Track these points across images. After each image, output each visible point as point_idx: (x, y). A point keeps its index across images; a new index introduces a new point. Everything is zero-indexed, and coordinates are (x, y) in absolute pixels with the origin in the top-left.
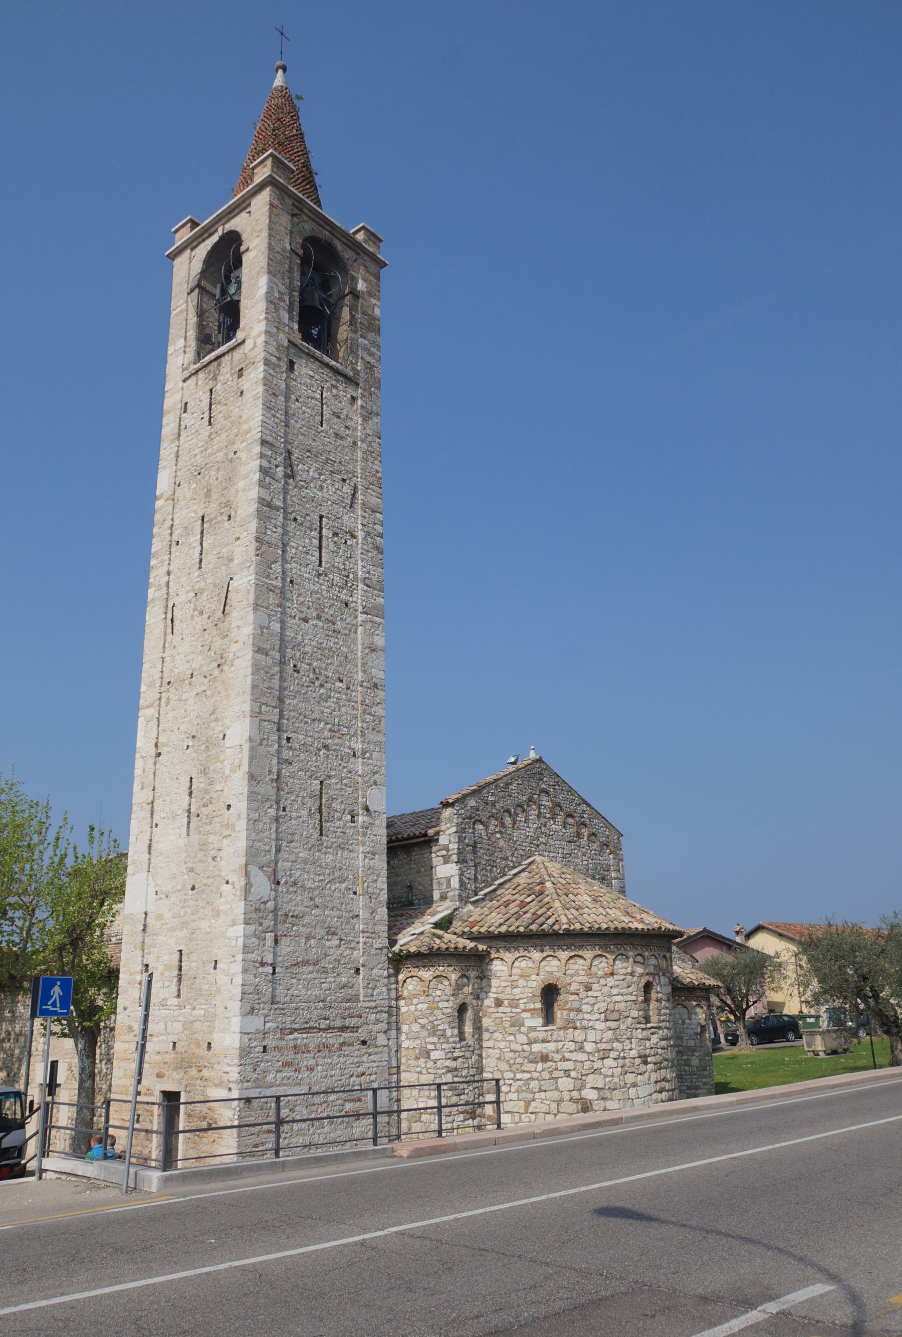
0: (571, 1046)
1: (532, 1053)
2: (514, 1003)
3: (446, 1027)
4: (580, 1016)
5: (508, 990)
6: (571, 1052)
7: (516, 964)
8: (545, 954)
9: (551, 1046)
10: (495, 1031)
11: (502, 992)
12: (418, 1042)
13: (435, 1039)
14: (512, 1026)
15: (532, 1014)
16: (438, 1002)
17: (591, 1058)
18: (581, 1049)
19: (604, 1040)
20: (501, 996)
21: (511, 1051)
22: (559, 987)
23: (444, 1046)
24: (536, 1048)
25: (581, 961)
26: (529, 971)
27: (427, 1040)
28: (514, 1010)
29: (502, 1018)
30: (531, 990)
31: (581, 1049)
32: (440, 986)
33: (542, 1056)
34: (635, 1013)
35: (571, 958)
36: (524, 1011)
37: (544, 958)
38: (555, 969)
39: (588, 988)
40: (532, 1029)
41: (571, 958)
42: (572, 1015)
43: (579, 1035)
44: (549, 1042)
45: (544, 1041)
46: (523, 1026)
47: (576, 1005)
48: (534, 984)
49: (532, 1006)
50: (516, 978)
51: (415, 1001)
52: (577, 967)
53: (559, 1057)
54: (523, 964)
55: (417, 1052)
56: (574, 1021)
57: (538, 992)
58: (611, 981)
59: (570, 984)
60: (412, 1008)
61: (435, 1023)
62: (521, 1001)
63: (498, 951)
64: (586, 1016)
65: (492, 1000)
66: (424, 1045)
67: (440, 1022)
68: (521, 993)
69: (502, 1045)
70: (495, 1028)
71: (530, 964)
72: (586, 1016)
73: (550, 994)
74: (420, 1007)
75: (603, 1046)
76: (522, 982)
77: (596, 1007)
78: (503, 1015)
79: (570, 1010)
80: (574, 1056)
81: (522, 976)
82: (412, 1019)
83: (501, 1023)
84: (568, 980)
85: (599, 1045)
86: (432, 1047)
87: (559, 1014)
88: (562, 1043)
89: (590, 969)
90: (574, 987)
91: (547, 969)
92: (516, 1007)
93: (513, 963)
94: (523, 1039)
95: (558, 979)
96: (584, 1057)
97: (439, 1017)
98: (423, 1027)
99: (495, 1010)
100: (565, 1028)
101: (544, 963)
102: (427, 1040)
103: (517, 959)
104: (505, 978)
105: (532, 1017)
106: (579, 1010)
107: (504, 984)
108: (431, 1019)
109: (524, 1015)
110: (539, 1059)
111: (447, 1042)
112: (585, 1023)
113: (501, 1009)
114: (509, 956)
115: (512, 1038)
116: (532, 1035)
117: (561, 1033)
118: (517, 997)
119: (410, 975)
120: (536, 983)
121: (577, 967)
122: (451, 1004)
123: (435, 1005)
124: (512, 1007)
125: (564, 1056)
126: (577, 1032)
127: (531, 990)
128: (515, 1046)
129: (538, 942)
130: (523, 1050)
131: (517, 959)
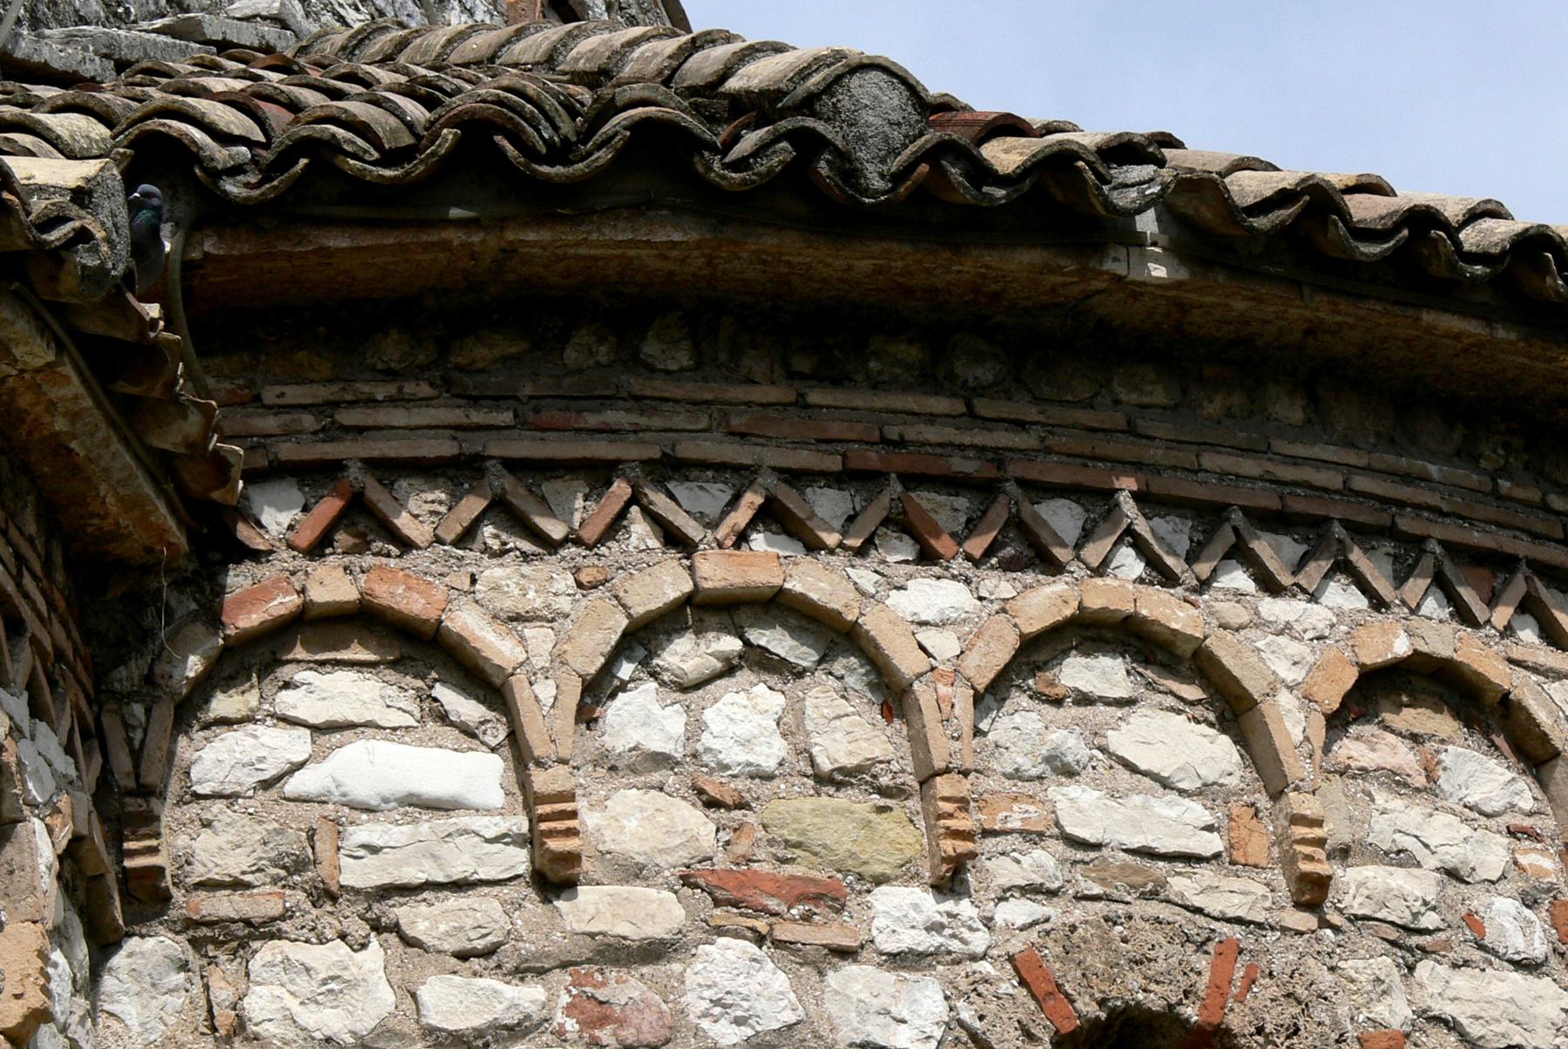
8: (1045, 601)
37: (1038, 651)
38: (1178, 824)
50: (657, 911)
52: (1445, 835)
54: (744, 723)
63: (365, 524)
71: (846, 729)
81: (724, 896)
91: (1082, 807)
93: (598, 690)
103: (644, 637)
104: (481, 915)
114: (523, 604)
129: (930, 421)
131: (644, 637)
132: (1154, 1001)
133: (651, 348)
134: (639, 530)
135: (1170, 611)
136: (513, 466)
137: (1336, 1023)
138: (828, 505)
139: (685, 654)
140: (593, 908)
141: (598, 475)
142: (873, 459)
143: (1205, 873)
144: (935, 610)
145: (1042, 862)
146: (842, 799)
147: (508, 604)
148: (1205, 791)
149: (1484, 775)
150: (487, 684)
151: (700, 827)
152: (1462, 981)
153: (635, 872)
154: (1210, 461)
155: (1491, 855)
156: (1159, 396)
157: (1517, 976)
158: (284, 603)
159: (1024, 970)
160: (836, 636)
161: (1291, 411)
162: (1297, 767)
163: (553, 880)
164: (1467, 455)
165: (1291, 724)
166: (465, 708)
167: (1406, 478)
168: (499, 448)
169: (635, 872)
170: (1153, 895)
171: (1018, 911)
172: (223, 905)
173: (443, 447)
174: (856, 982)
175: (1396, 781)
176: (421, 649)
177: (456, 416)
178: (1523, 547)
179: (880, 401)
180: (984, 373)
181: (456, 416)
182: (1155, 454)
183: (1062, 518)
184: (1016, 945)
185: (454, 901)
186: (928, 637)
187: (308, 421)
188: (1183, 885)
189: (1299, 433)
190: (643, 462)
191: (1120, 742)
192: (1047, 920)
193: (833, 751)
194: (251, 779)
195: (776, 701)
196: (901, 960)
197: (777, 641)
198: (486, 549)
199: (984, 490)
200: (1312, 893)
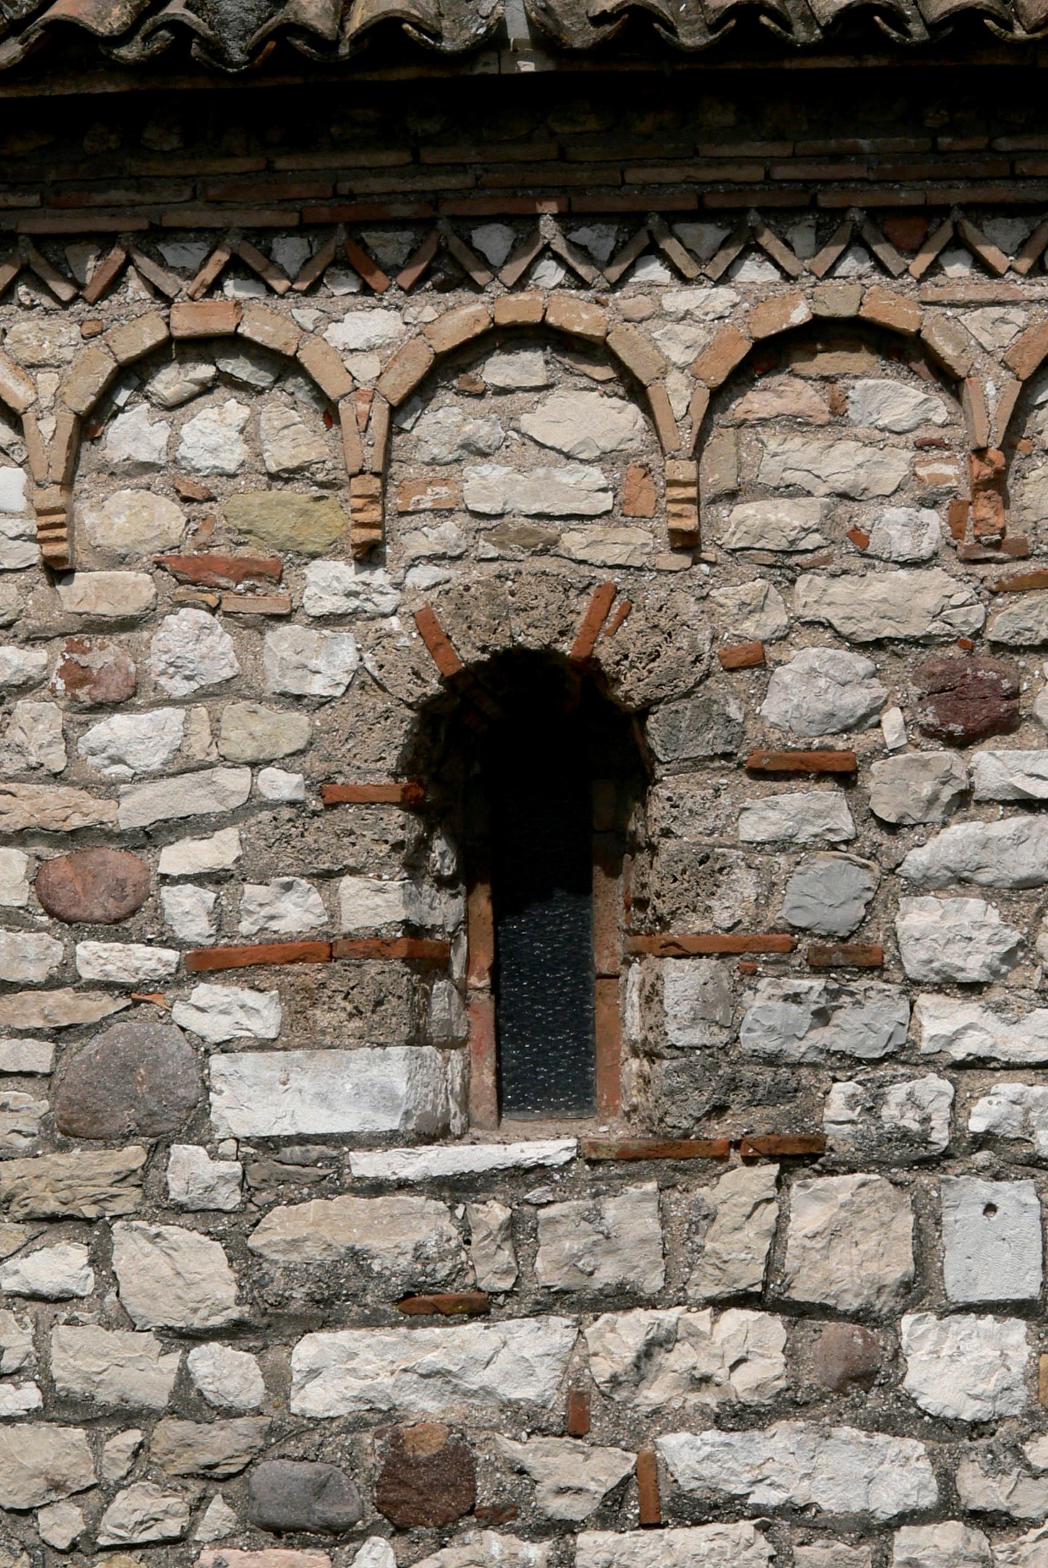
0: (752, 1351)
1: (283, 1431)
4: (867, 1020)
6: (739, 1417)
7: (134, 433)
8: (461, 316)
9: (518, 1358)
14: (66, 1131)
15: (300, 1006)
17: (978, 1488)
18: (862, 1387)
21: (61, 1407)
22: (632, 687)
24: (340, 1371)
25: (897, 399)
26: (282, 513)
28: (96, 957)
30: (296, 727)
31: (862, 1387)
33: (398, 1468)
35: (771, 355)
36: (204, 964)
37: (452, 366)
38: (580, 487)
41: (771, 355)
42: (772, 1014)
43: (841, 1235)
44: (479, 1308)
45: (425, 1301)
46: (195, 1124)
47: (823, 895)
48: (331, 664)
49: (296, 912)
50: (136, 588)
52: (841, 462)
53: (601, 1468)
54: (214, 433)
56: (785, 1079)
57: (377, 753)
59: (755, 662)
62: (175, 858)
64: (942, 1021)
68: (182, 766)
71: (290, 433)
72: (942, 1021)
73: (529, 779)
79: (748, 952)
80: (779, 1463)
81: (190, 575)
84: (744, 606)
87: (659, 1002)
88: (623, 1334)
89: (996, 485)
90: (808, 690)
91: (488, 485)
92: (114, 928)
93: (90, 424)
94: (181, 1271)
95: (610, 602)
96: (899, 1475)
100: (673, 1156)
101: (445, 420)
103: (134, 372)
105: (299, 1034)
106: (851, 958)
109: (217, 1009)
110: (353, 1501)
112: (920, 1101)
115: (60, 1265)
116: (302, 1231)
117: (633, 1211)
118: (137, 809)
120: (345, 650)
121: (841, 462)
124: (70, 923)
125: (650, 1467)
126: (815, 1204)
127: (296, 727)
128: (84, 1356)
129: (378, 173)
130: (188, 1402)
131: (134, 372)
132: (533, 640)
133: (150, 134)
134: (134, 286)
135: (579, 315)
136: (39, 241)
137: (693, 646)
138: (289, 251)
139: (169, 381)
140: (85, 593)
141: (105, 241)
142: (324, 214)
143: (596, 529)
144: (364, 334)
146: (287, 492)
147: (26, 355)
152: (840, 588)
153: (120, 561)
154: (632, 176)
156: (592, 124)
157: (903, 574)
159: (425, 623)
160: (285, 366)
163: (58, 571)
167: (836, 158)
168: (27, 226)
170: (544, 552)
171: (423, 576)
174: (282, 641)
179: (336, 162)
180: (431, 126)
182: (582, 176)
183: (493, 240)
184: (418, 605)
186: (354, 363)
188: (574, 541)
190: (134, 232)
191: (533, 423)
192: (447, 582)
193: (280, 454)
195: (245, 412)
196: (324, 620)
197: (240, 368)
198: (21, 305)
199: (424, 225)
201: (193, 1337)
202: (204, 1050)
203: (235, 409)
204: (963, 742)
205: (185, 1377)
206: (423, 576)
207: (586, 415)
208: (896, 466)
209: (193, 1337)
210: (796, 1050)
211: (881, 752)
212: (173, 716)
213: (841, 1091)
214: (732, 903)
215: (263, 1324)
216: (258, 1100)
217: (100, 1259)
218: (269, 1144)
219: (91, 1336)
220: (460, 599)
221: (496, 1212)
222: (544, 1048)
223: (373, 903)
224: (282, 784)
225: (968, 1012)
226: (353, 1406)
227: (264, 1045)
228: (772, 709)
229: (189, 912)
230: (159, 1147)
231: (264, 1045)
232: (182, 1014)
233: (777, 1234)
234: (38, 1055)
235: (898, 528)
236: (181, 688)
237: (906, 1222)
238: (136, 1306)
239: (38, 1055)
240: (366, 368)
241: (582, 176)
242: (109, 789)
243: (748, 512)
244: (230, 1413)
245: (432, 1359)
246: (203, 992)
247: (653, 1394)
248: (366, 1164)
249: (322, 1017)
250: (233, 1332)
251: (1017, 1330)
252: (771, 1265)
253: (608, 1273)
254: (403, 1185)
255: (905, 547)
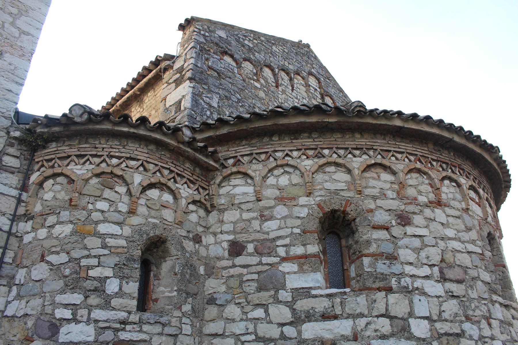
2: (266, 247)
3: (109, 272)
4: (397, 268)
5: (256, 224)
7: (271, 180)
10: (228, 302)
11: (245, 230)
12: (36, 302)
13: (77, 298)
14: (260, 289)
15: (301, 266)
16: (97, 223)
19: (445, 315)
20: (242, 238)
22: (352, 214)
23: (98, 314)
26: (294, 191)
27: (60, 299)
28: (265, 260)
29: (241, 275)
32: (107, 193)
34: (486, 277)
35: (369, 167)
36: (284, 259)
38: (341, 186)
39: (404, 220)
40: (304, 293)
41: (369, 167)
42: (382, 267)
43: (398, 304)
44: (336, 317)
45: (326, 317)
46: (283, 287)
48: (304, 212)
49: (299, 250)
50: (272, 203)
51: (51, 220)
52: (380, 184)
54: (284, 181)
55: (30, 323)
56: (384, 277)
58: (439, 214)
60: (42, 233)
61: (84, 262)
62: (279, 243)
64: (408, 269)
65: (225, 245)
66: (48, 309)
67: (94, 262)
68: (280, 228)
69: (239, 328)
70: (229, 297)
72: (408, 269)
74: (58, 229)
75: (442, 327)
76: (281, 211)
77: (423, 254)
78: (245, 271)
81: (281, 200)
82: (37, 256)
83: (241, 285)
85: (438, 325)
86: (67, 314)
88: (362, 322)
91: (328, 185)
92: (269, 255)
93: (265, 178)
95: (348, 202)
97: (94, 252)
98: (55, 269)
99: (229, 263)
102: (60, 299)
103: (271, 170)
104: (250, 206)
105: (301, 270)
107: (246, 216)
108: (76, 254)
109: (287, 267)
111: (107, 305)
112: (406, 281)
113: (240, 260)
114: (256, 169)
115: (259, 313)
117: (362, 299)
118: (272, 236)
119: (50, 172)
121: (380, 184)
122: (127, 231)
123: (90, 228)
126: (392, 298)
127: (298, 222)
131: (271, 170)
133: (274, 138)
136: (257, 154)
137: (362, 208)
139: (276, 172)
142: (300, 148)
143: (345, 192)
145: (322, 193)
146: (296, 187)
147: (254, 169)
148: (345, 182)
149: (386, 176)
150: (252, 178)
151: (278, 192)
152: (383, 202)
153: (269, 199)
154: (346, 143)
155: (388, 186)
156: (340, 136)
157: (391, 201)
158: (229, 172)
159: (319, 206)
160: (295, 168)
161: (358, 136)
162: (357, 178)
164: (384, 139)
165: (356, 172)
166: (249, 181)
168: (255, 152)
169: (269, 199)
170: (337, 195)
172: (221, 207)
173: (249, 152)
175: (374, 179)
176: (246, 175)
177: (250, 149)
178: (392, 149)
179: (302, 141)
180: (316, 136)
181: (250, 149)
182: (338, 143)
184: (318, 203)
185: (247, 204)
186: (306, 167)
187: (234, 152)
188: (342, 193)
189: (361, 138)
191: (333, 177)
193: (294, 181)
194: (225, 192)
195: (288, 177)
196: (302, 206)
200: (360, 192)
201: (282, 325)
202: (284, 274)
203: (287, 177)
204: (404, 226)
205: (282, 332)
206: (318, 199)
207: (342, 176)
208: (388, 186)
209: (282, 325)
210: (385, 272)
211: (393, 226)
212: (278, 221)
213: (394, 280)
214: (373, 249)
215: (297, 321)
216: (295, 282)
217: (266, 311)
218: (297, 289)
219: (265, 325)
220: (325, 202)
221: (338, 300)
222: (338, 278)
223: (314, 249)
224: (297, 231)
225: (411, 267)
226: (314, 336)
227: (295, 273)
228: (375, 219)
229: (281, 251)
230: (277, 292)
231: (295, 273)
232: (280, 268)
233: (387, 305)
234: (255, 276)
235: (391, 194)
236: (279, 217)
237: (407, 302)
238: (273, 319)
239: (255, 276)
240: (308, 168)
241: (338, 143)
242: (268, 233)
243: (369, 190)
244: (291, 339)
245: (328, 327)
246: (284, 264)
247: (368, 333)
248: (314, 292)
249: (305, 267)
250: (291, 324)
251: (426, 322)
252: (387, 310)
253: (358, 311)
254: (321, 296)
255: (391, 197)
